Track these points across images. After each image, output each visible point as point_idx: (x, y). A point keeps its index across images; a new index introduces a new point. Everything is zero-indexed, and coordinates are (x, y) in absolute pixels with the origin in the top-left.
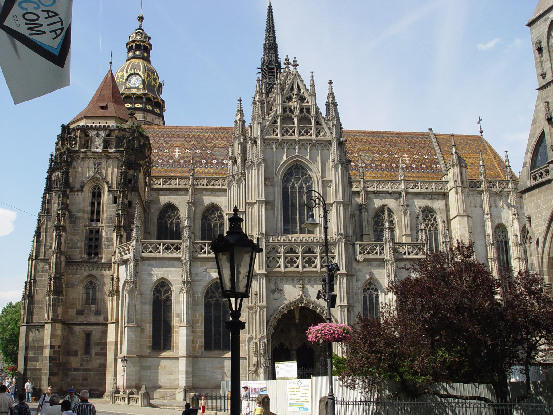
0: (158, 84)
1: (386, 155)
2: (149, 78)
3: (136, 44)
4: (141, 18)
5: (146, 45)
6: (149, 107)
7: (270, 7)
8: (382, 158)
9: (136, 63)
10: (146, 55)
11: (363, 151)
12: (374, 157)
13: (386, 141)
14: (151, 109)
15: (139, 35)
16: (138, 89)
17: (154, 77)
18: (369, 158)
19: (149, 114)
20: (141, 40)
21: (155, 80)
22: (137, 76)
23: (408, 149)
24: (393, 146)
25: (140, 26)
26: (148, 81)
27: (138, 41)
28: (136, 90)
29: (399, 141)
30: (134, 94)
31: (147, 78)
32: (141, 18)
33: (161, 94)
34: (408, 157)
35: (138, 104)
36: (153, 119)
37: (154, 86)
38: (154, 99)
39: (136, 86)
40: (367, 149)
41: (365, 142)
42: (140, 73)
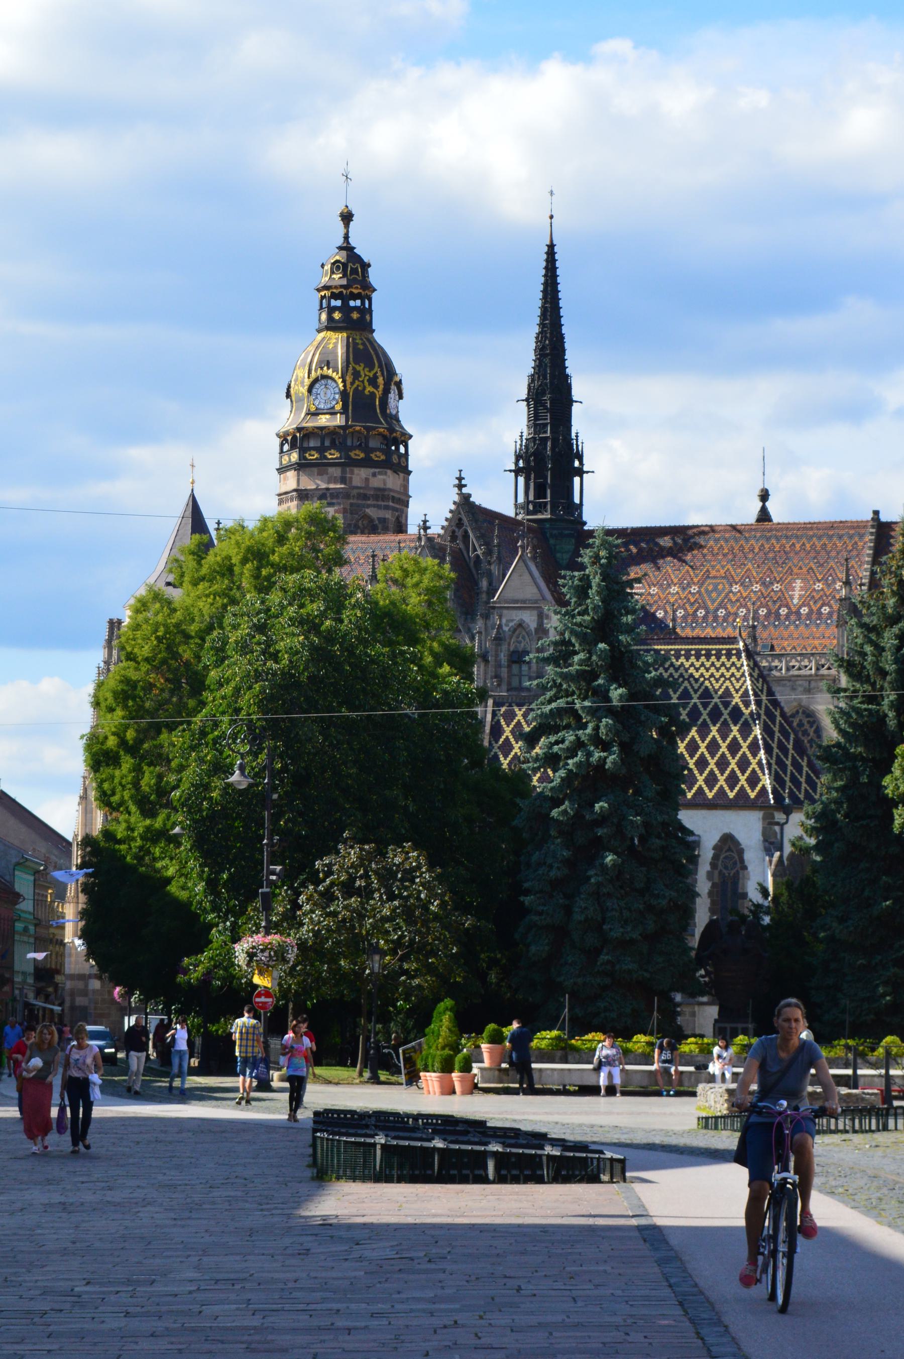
0: (381, 387)
1: (756, 587)
2: (357, 383)
4: (347, 218)
7: (551, 247)
8: (745, 595)
11: (715, 577)
12: (731, 591)
13: (772, 548)
14: (362, 455)
17: (371, 375)
18: (719, 595)
19: (356, 470)
21: (373, 382)
22: (330, 381)
23: (811, 568)
24: (780, 562)
25: (346, 237)
26: (356, 389)
27: (336, 287)
28: (328, 416)
29: (798, 546)
30: (322, 428)
31: (352, 383)
32: (347, 218)
33: (401, 397)
34: (802, 589)
36: (367, 480)
37: (372, 395)
38: (368, 432)
40: (722, 572)
41: (725, 555)
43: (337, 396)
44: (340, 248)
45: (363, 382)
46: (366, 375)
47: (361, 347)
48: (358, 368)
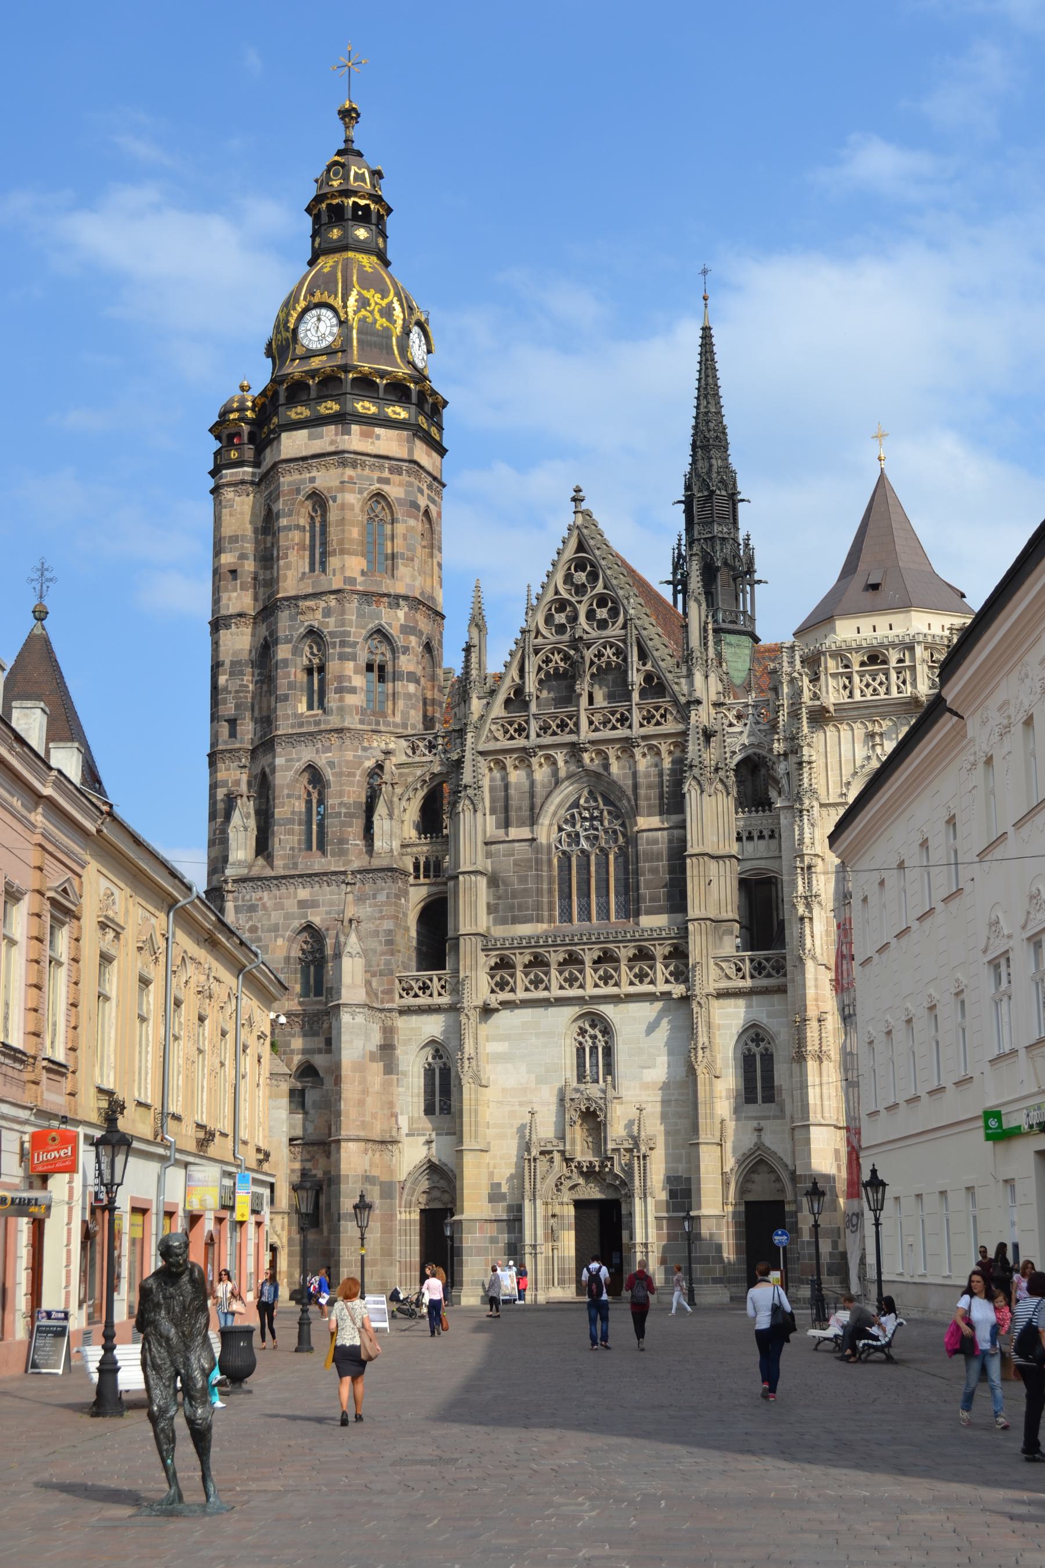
0: (400, 322)
2: (363, 312)
3: (329, 205)
5: (362, 202)
6: (365, 407)
9: (326, 270)
10: (362, 233)
14: (373, 409)
15: (336, 174)
16: (329, 352)
17: (384, 303)
20: (342, 188)
21: (387, 312)
22: (324, 311)
26: (363, 321)
28: (324, 358)
30: (313, 373)
31: (355, 313)
32: (348, 115)
35: (329, 404)
37: (387, 333)
39: (324, 344)
42: (331, 301)
43: (335, 330)
44: (340, 153)
45: (372, 312)
46: (377, 304)
47: (370, 270)
48: (364, 293)
